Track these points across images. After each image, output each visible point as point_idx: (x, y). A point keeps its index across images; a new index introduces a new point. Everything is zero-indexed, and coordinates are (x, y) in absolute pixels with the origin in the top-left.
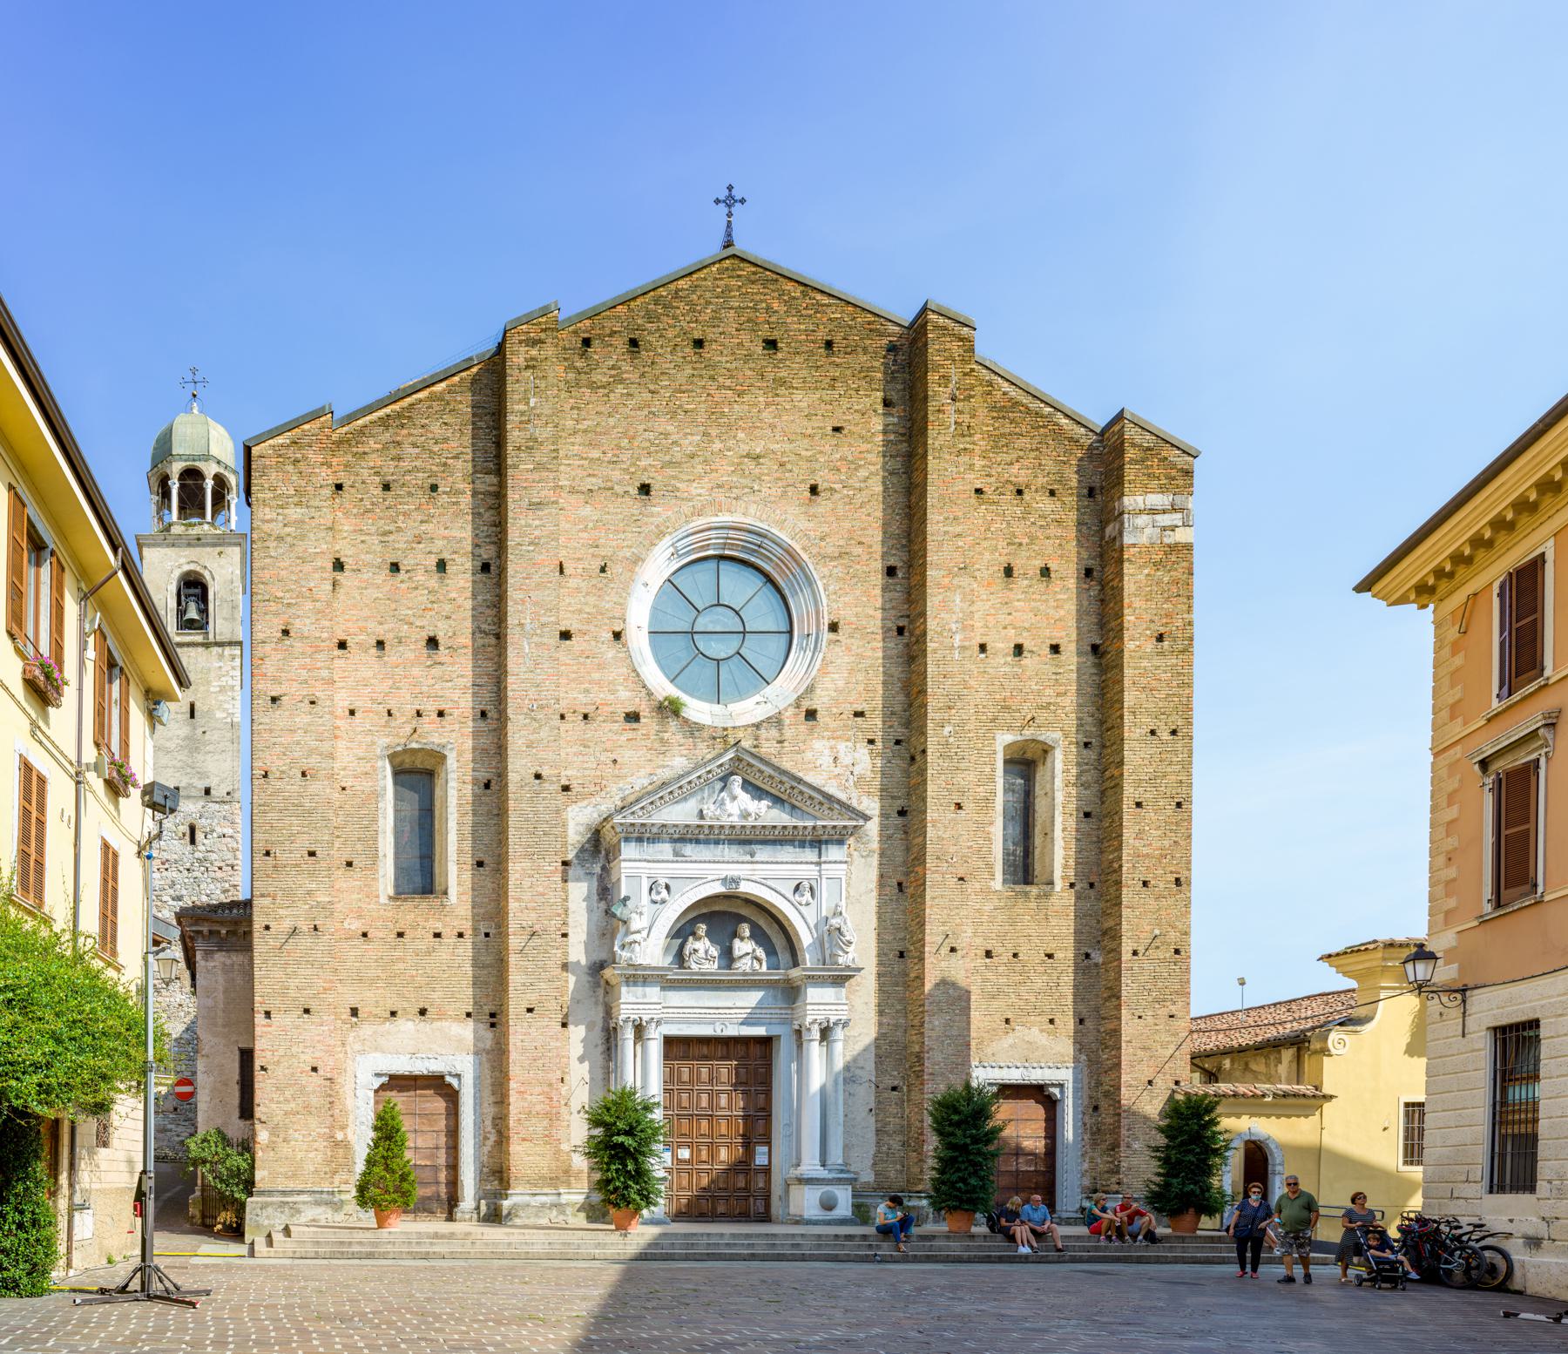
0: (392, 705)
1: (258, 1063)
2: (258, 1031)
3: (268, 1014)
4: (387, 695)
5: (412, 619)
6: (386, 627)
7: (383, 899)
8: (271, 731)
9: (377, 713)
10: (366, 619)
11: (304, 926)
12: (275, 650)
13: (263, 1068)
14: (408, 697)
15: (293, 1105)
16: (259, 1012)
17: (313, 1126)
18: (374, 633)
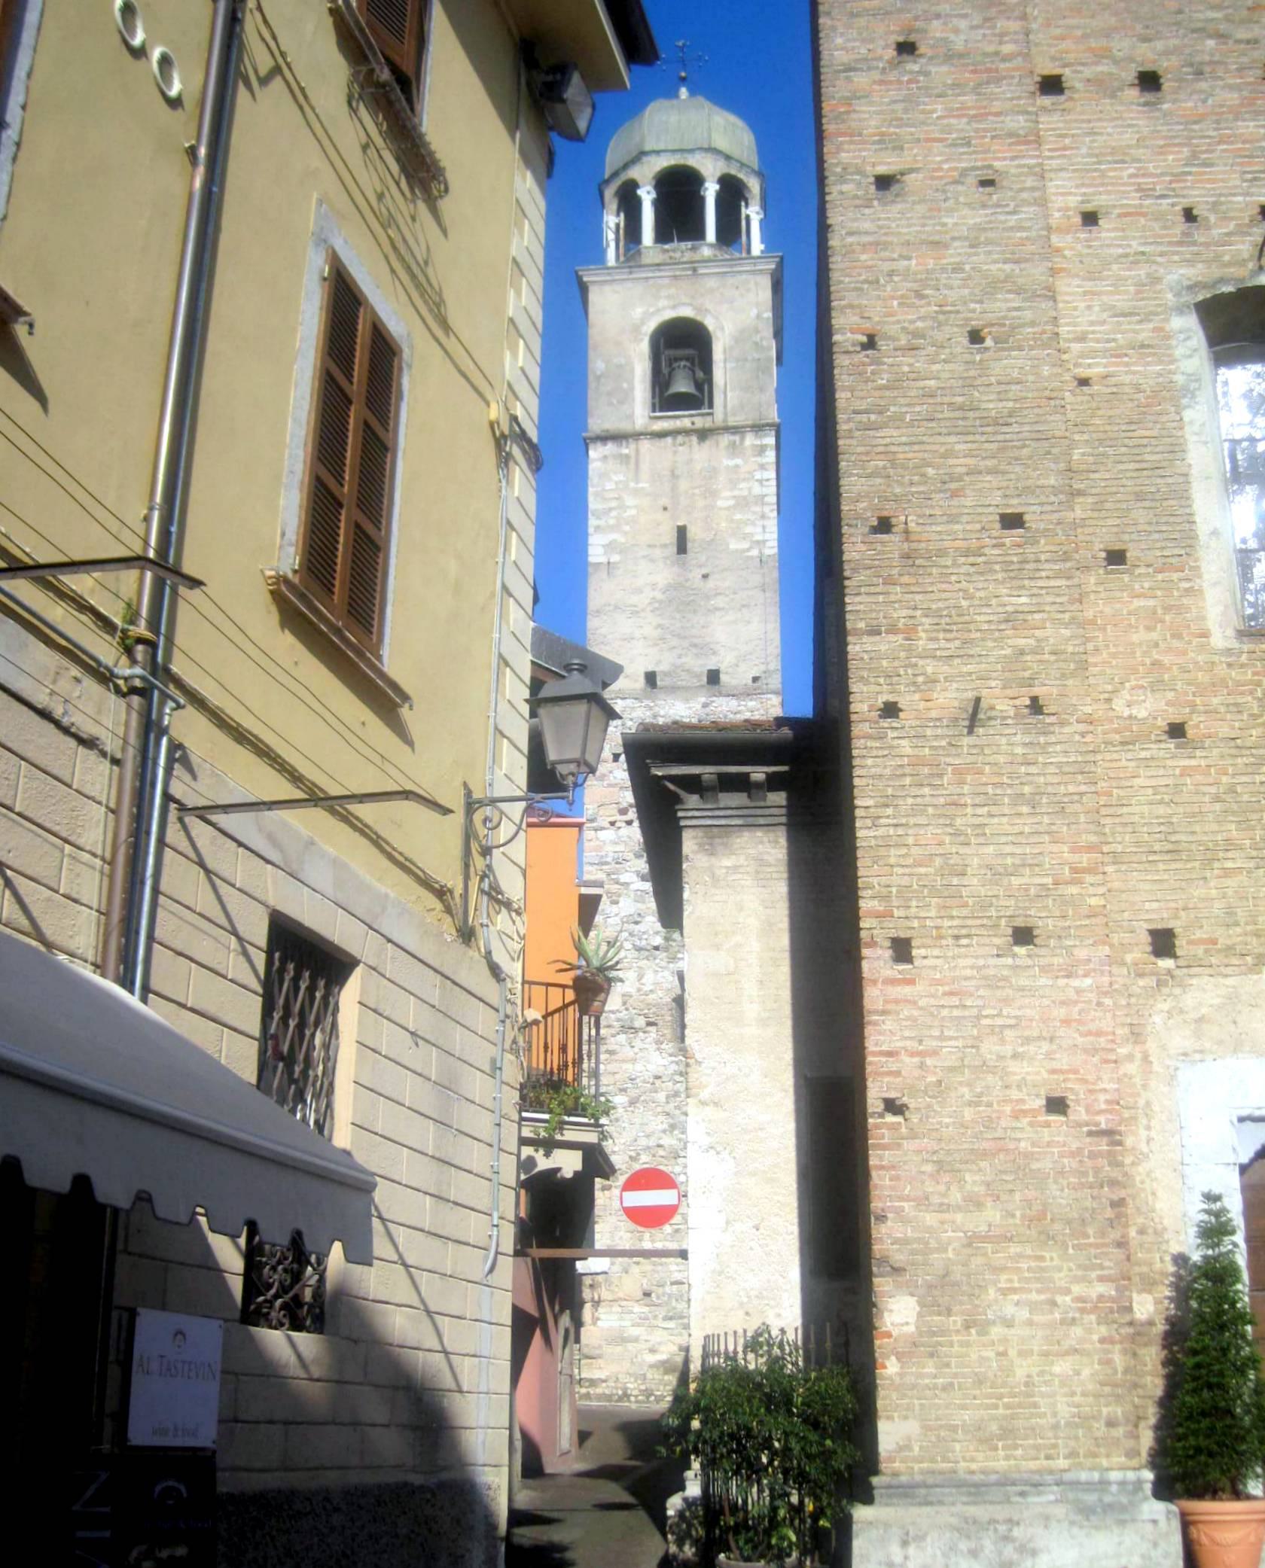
0: (1197, 197)
1: (875, 1093)
2: (873, 996)
3: (902, 950)
4: (1179, 177)
5: (1222, 27)
6: (1159, 45)
7: (1222, 637)
8: (877, 246)
9: (1159, 217)
10: (1107, 33)
11: (1002, 703)
12: (881, 82)
13: (892, 1106)
14: (1235, 180)
15: (992, 1214)
16: (873, 944)
17: (1060, 1278)
18: (1131, 60)
